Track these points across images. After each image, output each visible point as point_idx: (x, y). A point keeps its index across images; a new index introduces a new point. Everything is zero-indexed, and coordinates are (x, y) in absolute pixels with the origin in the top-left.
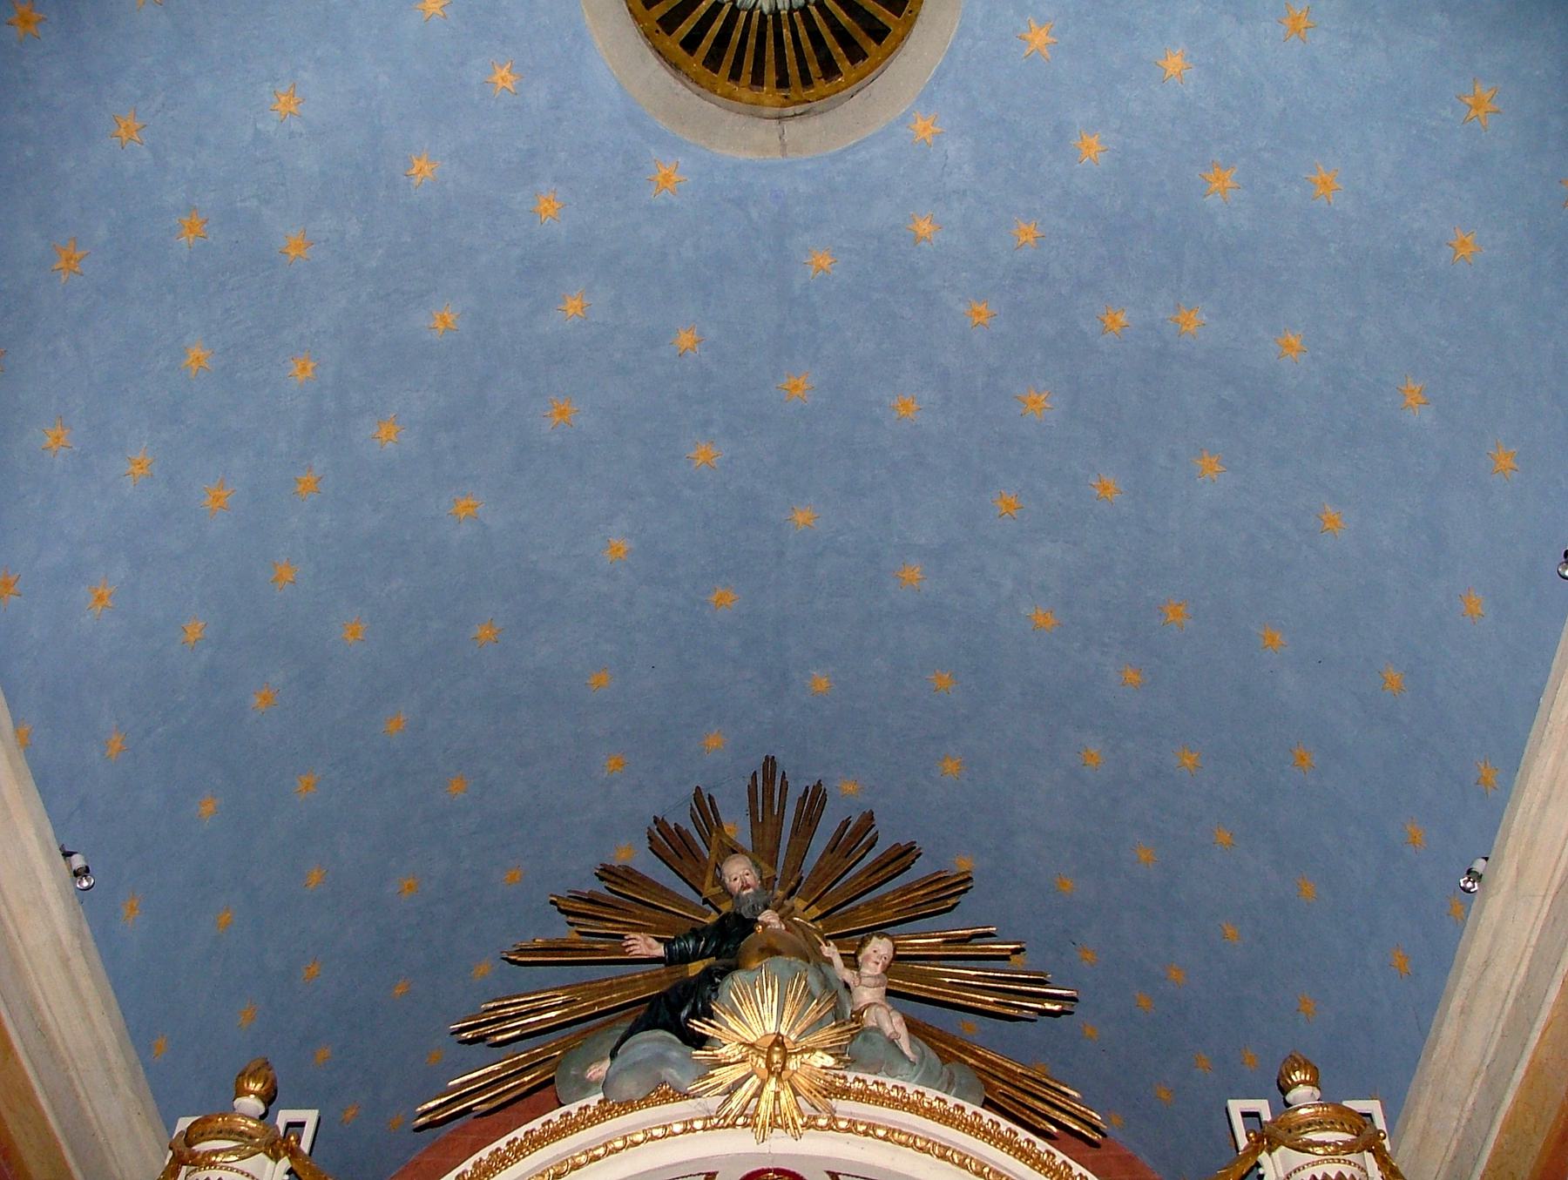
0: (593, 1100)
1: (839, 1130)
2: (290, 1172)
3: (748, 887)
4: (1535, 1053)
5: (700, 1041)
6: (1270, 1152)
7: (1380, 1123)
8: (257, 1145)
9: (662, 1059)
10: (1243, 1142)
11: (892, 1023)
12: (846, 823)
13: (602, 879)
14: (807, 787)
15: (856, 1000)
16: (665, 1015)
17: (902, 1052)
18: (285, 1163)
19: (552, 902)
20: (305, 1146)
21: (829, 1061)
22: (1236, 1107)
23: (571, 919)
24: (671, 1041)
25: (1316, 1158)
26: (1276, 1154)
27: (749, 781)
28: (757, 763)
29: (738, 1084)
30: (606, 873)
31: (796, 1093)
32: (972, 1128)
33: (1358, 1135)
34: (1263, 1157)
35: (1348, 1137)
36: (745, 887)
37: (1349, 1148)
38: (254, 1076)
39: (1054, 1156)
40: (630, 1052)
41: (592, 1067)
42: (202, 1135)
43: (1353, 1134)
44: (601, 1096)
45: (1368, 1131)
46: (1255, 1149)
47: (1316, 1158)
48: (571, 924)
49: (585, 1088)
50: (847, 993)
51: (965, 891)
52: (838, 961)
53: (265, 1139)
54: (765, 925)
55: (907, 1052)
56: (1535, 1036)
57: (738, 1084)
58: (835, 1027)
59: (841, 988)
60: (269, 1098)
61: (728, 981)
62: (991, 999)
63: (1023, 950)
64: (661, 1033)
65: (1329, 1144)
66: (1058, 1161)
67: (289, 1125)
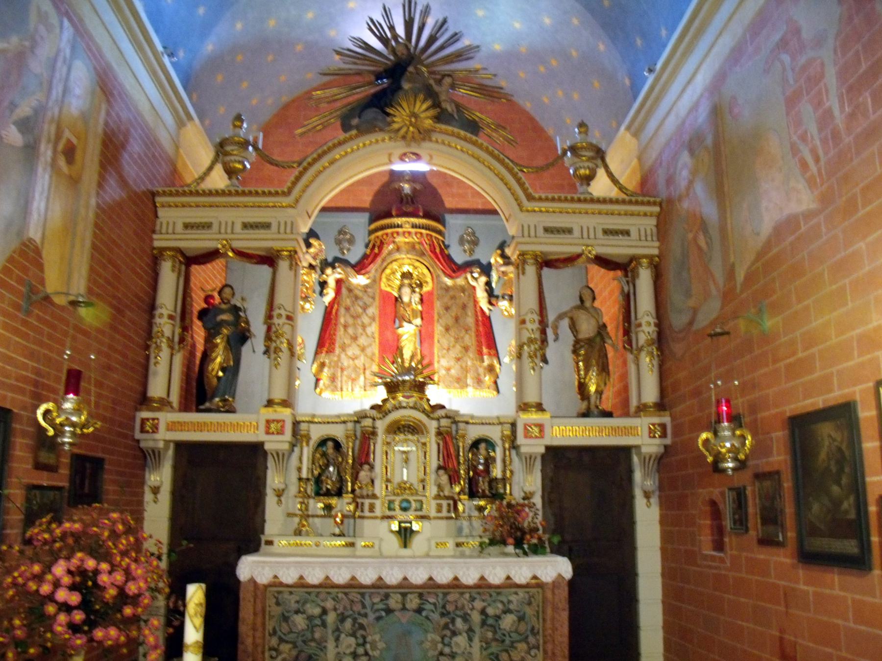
5: (388, 114)
9: (375, 119)
21: (431, 121)
29: (399, 130)
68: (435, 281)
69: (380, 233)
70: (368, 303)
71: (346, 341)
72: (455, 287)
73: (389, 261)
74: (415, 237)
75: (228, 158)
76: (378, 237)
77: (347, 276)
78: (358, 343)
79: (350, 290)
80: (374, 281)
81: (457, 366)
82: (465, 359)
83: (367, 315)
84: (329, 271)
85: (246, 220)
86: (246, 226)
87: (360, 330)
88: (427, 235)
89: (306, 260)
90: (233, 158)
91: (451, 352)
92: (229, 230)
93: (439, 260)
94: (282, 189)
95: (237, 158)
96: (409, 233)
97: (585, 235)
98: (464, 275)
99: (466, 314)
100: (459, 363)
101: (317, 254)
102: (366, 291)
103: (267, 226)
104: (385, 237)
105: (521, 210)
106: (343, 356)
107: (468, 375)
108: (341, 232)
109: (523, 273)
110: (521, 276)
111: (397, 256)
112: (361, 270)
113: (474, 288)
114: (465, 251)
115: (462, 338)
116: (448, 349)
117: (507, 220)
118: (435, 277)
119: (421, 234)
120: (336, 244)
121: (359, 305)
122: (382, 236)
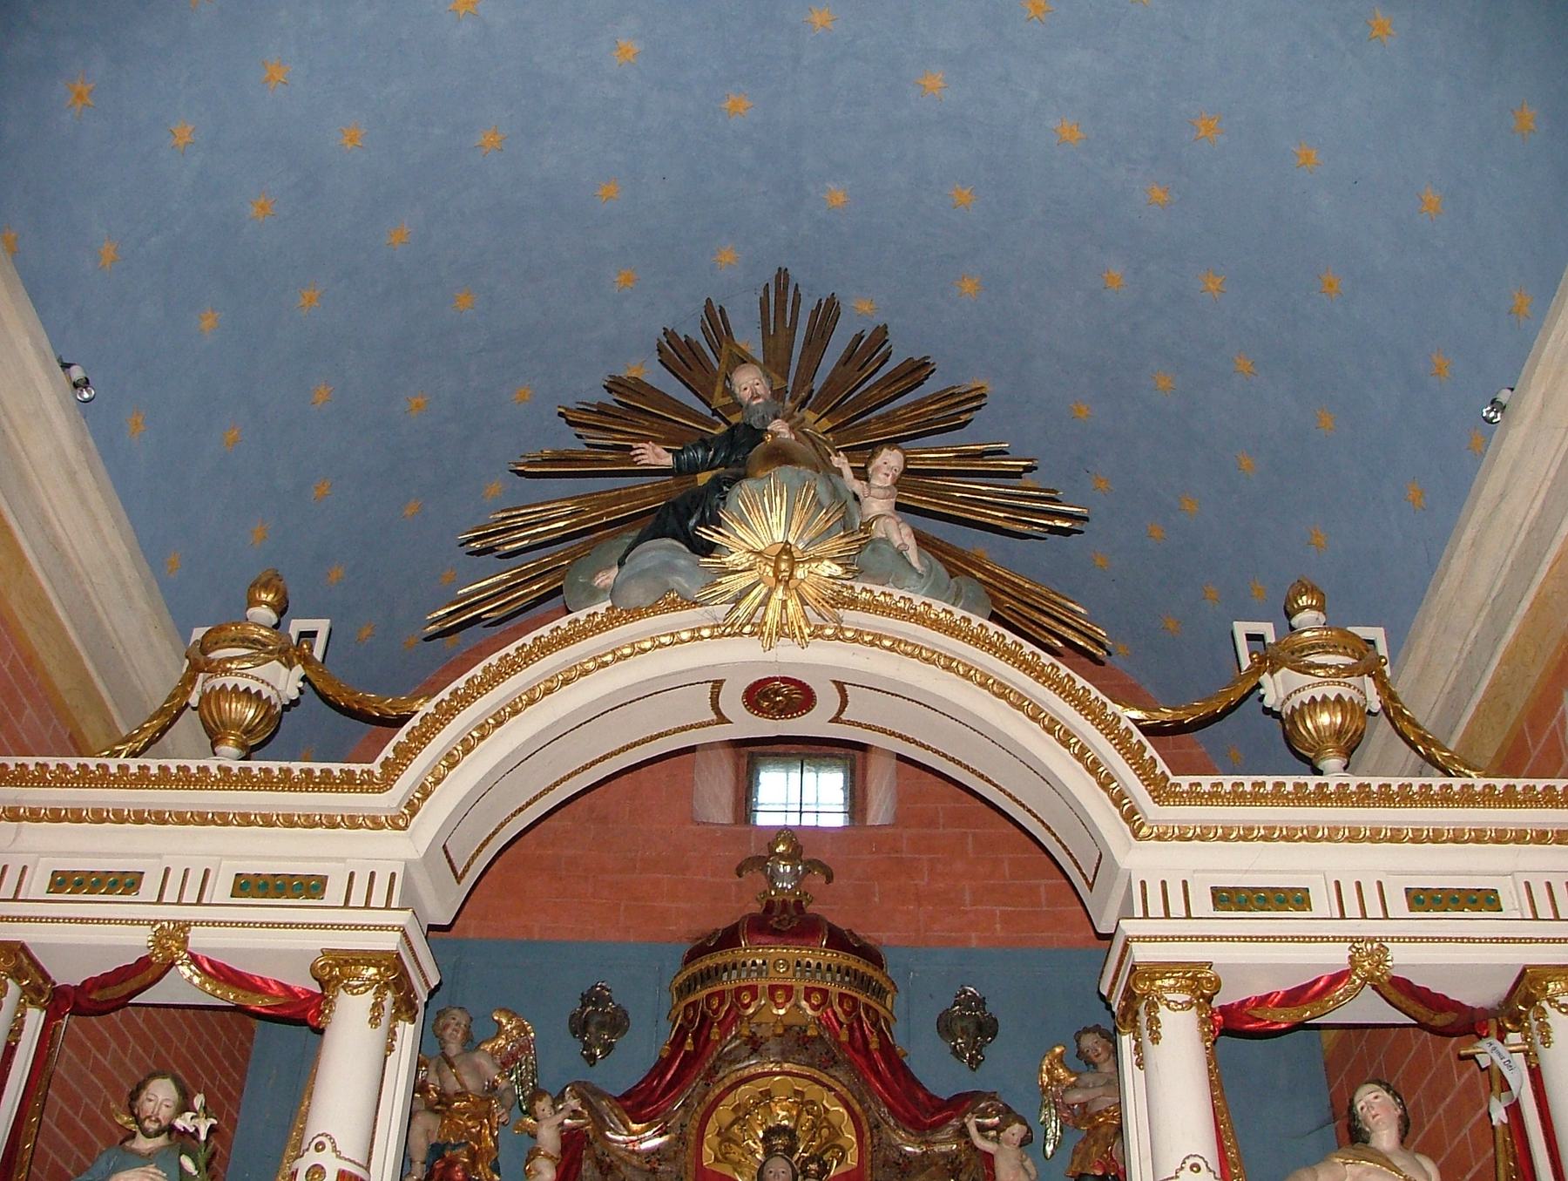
0: (601, 607)
1: (845, 639)
2: (304, 679)
3: (758, 397)
4: (1543, 585)
5: (708, 549)
6: (1272, 674)
7: (1382, 649)
8: (271, 652)
9: (672, 569)
10: (1246, 663)
11: (900, 534)
12: (860, 337)
13: (610, 391)
14: (820, 300)
15: (866, 510)
16: (672, 523)
17: (910, 564)
18: (299, 671)
19: (561, 414)
20: (318, 654)
21: (837, 570)
22: (1241, 629)
23: (579, 431)
24: (681, 550)
25: (1318, 680)
26: (1277, 675)
27: (761, 293)
28: (769, 275)
29: (746, 592)
30: (616, 384)
31: (804, 602)
32: (978, 640)
33: (1360, 659)
34: (1265, 678)
35: (1350, 661)
36: (755, 396)
37: (1350, 671)
38: (266, 587)
39: (1058, 669)
40: (638, 560)
41: (600, 575)
42: (216, 643)
43: (1355, 658)
44: (609, 603)
45: (1369, 656)
46: (1257, 670)
47: (1318, 680)
48: (579, 436)
49: (593, 595)
50: (856, 504)
51: (978, 408)
52: (848, 472)
53: (278, 647)
54: (774, 434)
55: (916, 564)
56: (1544, 569)
57: (746, 592)
58: (844, 537)
59: (851, 497)
60: (282, 609)
61: (737, 489)
62: (1002, 515)
63: (1036, 468)
64: (668, 541)
65: (1331, 667)
66: (1062, 674)
67: (302, 635)
69: (701, 994)
72: (924, 1161)
73: (727, 1082)
74: (804, 1003)
75: (218, 682)
76: (694, 1004)
77: (601, 1125)
79: (605, 1168)
80: (681, 1139)
84: (543, 1106)
85: (251, 868)
86: (246, 886)
88: (842, 996)
89: (477, 1069)
90: (230, 681)
92: (191, 895)
93: (877, 1073)
94: (366, 767)
95: (243, 683)
96: (789, 991)
97: (1352, 908)
98: (954, 1122)
101: (513, 1057)
102: (654, 1171)
103: (312, 887)
104: (715, 1003)
105: (1135, 835)
108: (586, 999)
109: (1156, 1039)
110: (1147, 1043)
111: (753, 1065)
112: (642, 1105)
113: (988, 1158)
114: (958, 1054)
117: (1091, 886)
118: (866, 1128)
119: (824, 993)
120: (574, 1033)
122: (709, 997)
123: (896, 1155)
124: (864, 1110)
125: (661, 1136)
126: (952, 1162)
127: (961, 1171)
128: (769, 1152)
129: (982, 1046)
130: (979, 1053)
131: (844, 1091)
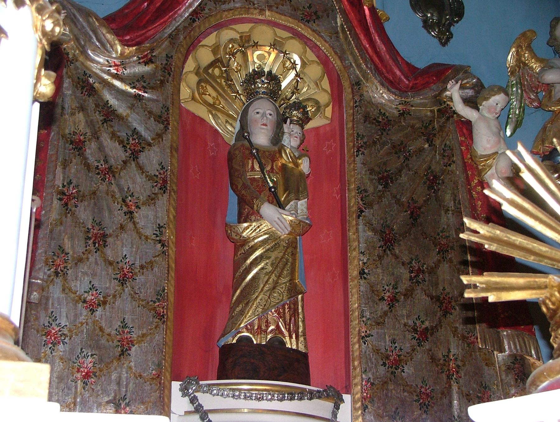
68: (347, 94)
70: (147, 135)
71: (67, 245)
78: (109, 252)
80: (167, 69)
81: (420, 356)
82: (442, 333)
83: (141, 168)
87: (120, 217)
91: (401, 310)
99: (439, 201)
100: (427, 346)
106: (56, 291)
107: (455, 388)
113: (468, 124)
114: (427, 25)
115: (432, 271)
116: (394, 300)
118: (346, 84)
121: (114, 136)
123: (376, 113)
124: (345, 67)
125: (146, 63)
126: (426, 127)
127: (435, 135)
128: (252, 95)
129: (450, 25)
130: (448, 30)
131: (325, 48)
